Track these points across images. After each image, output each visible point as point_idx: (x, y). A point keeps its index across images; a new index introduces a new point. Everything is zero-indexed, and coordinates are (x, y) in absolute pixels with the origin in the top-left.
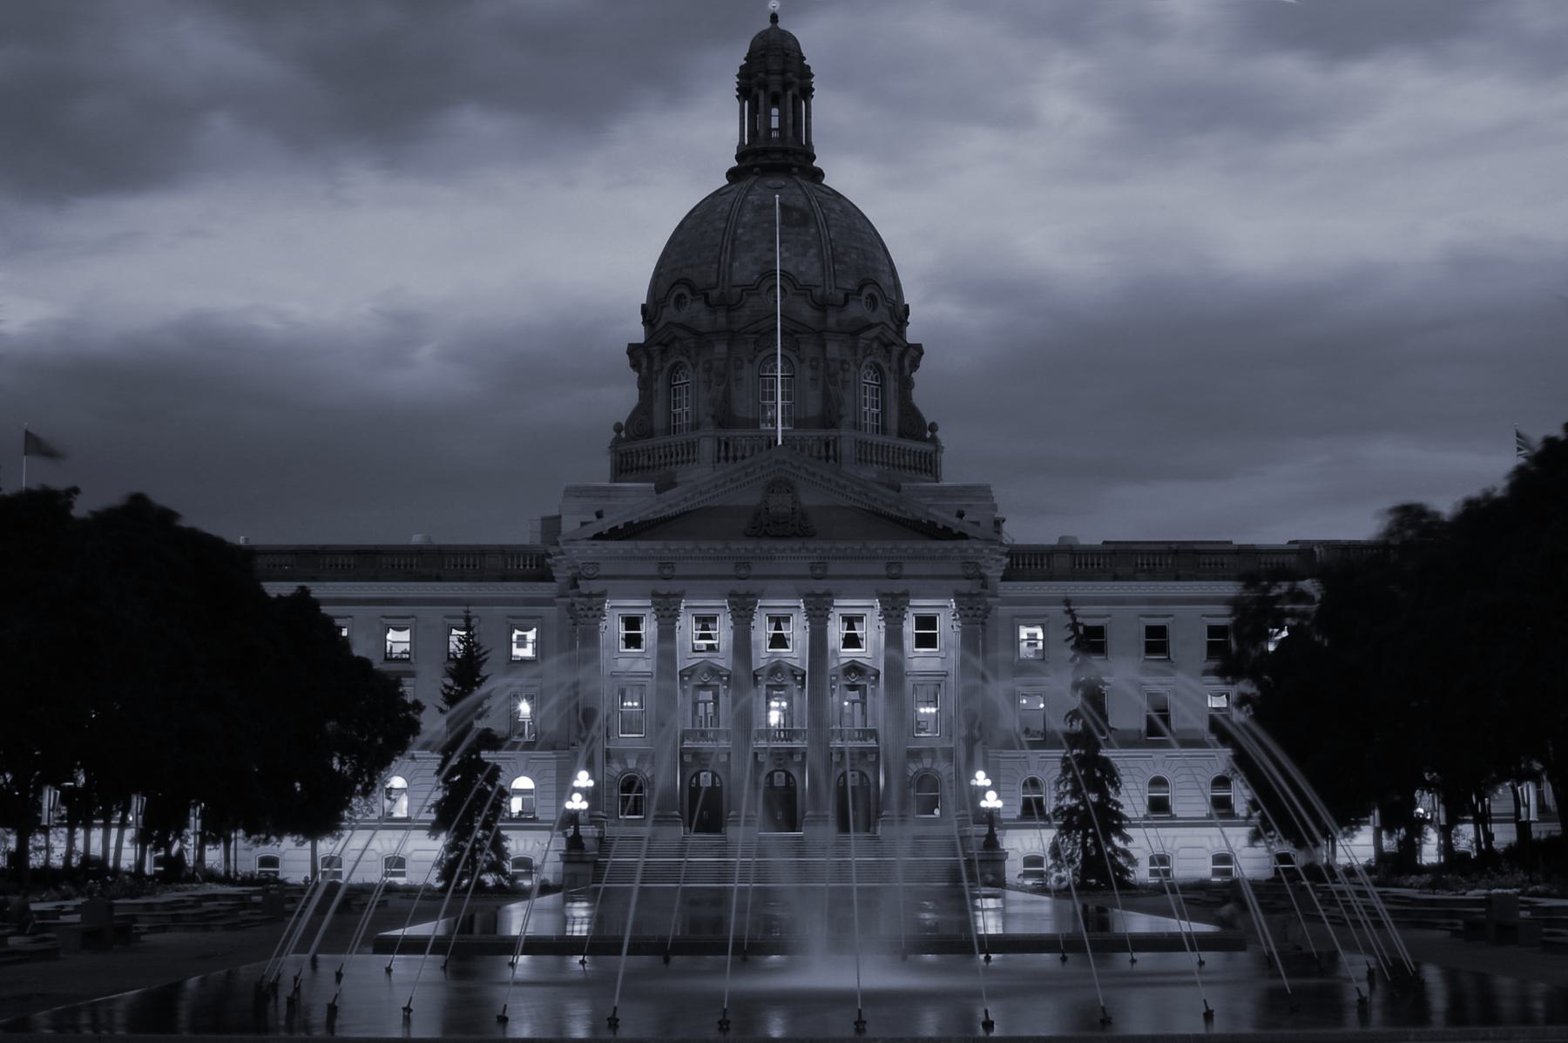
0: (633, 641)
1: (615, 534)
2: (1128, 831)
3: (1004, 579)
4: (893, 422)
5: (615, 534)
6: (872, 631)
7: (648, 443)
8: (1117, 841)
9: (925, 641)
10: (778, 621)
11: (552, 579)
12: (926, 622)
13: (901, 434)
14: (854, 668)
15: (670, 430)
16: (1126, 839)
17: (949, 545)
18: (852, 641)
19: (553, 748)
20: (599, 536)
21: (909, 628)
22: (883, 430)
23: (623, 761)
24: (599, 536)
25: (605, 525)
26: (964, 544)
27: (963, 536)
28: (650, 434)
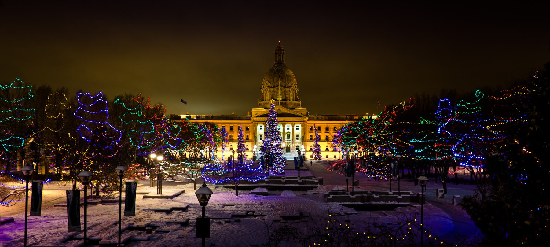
0: (261, 129)
1: (259, 116)
2: (321, 153)
3: (308, 120)
4: (295, 99)
5: (259, 116)
6: (291, 127)
7: (263, 102)
8: (320, 154)
9: (297, 129)
10: (279, 126)
11: (251, 120)
12: (297, 126)
13: (296, 101)
14: (288, 132)
15: (266, 100)
16: (321, 154)
17: (300, 118)
18: (288, 129)
19: (251, 141)
20: (257, 117)
21: (295, 128)
22: (293, 100)
23: (260, 143)
24: (257, 117)
25: (257, 115)
26: (302, 118)
27: (301, 117)
28: (263, 101)
